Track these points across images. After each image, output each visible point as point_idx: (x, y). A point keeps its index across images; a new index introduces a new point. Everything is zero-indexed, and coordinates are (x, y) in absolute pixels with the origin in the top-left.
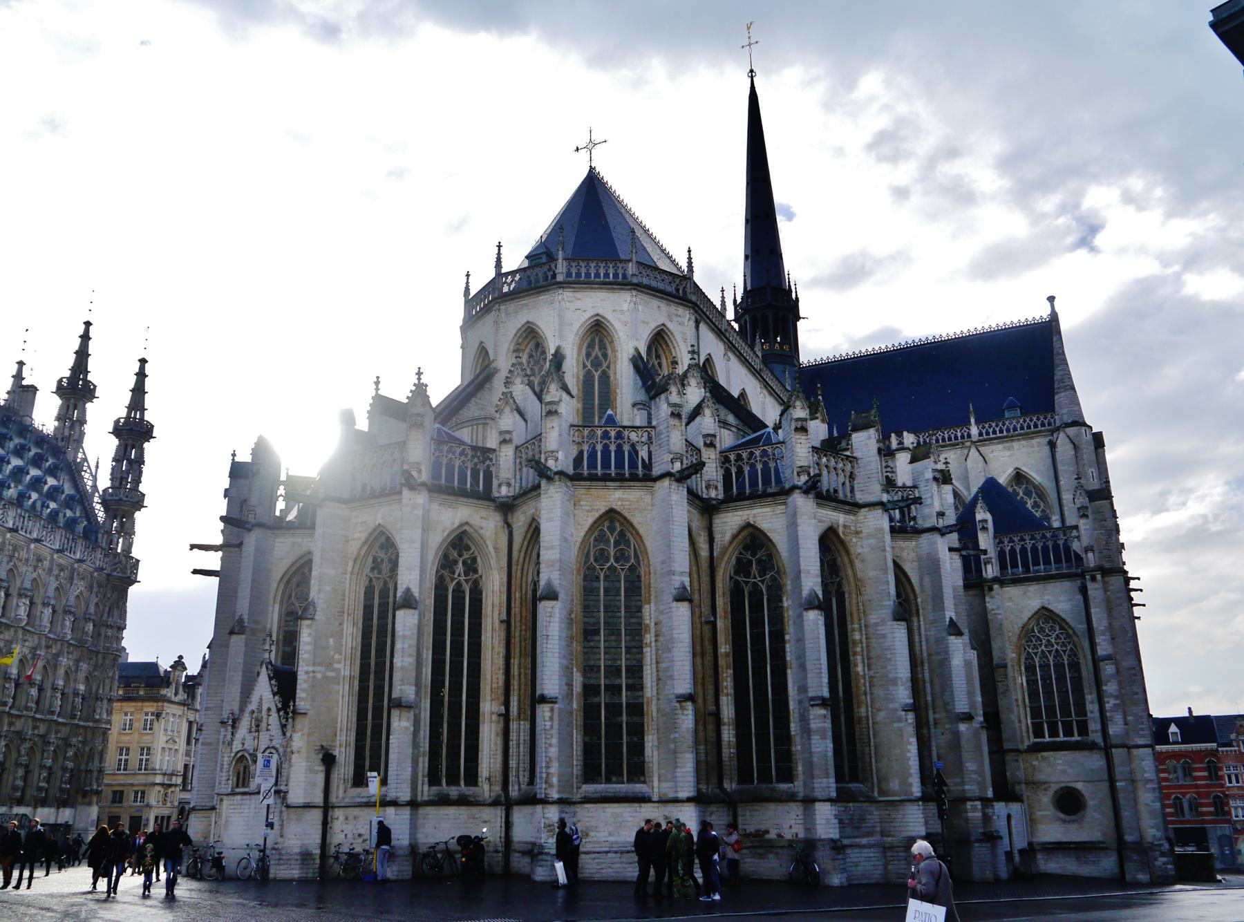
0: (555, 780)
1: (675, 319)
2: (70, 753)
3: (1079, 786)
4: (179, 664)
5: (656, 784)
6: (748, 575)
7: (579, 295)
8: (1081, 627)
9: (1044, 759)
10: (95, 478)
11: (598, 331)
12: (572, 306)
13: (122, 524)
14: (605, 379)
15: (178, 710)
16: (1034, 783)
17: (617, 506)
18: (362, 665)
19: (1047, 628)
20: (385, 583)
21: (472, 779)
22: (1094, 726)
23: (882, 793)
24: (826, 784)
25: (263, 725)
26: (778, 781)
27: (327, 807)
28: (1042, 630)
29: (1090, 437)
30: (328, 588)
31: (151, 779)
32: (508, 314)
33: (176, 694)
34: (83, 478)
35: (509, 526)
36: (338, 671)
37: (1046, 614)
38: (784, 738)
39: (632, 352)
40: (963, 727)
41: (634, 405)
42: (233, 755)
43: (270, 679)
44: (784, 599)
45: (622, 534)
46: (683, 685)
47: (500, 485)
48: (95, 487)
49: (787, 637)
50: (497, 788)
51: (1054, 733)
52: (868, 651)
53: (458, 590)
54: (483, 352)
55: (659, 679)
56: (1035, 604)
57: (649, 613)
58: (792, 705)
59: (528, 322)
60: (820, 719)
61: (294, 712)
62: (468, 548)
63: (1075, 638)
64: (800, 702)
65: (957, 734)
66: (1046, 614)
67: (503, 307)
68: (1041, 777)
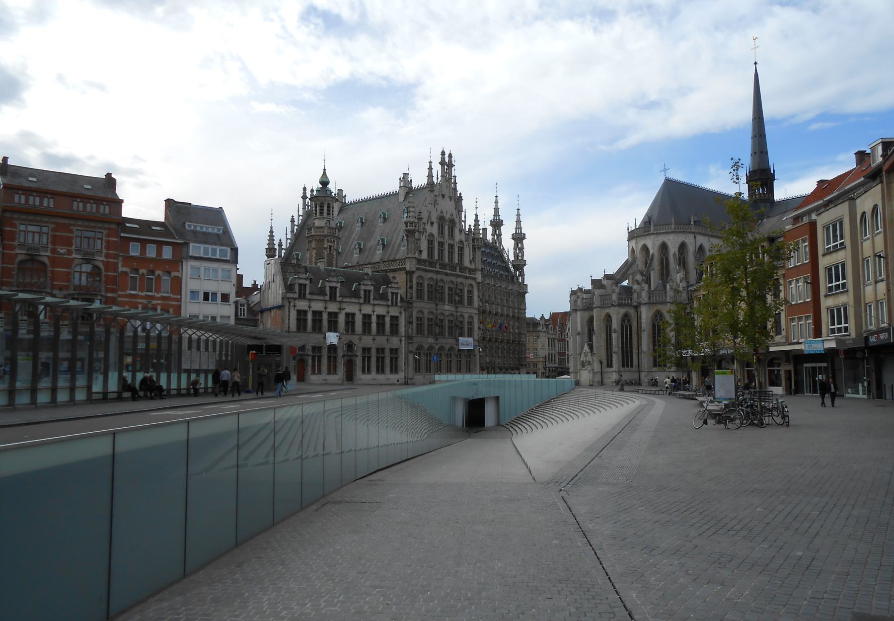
0: (646, 367)
2: (516, 353)
4: (542, 317)
7: (658, 236)
10: (508, 256)
11: (664, 247)
13: (520, 272)
14: (667, 259)
15: (544, 334)
17: (659, 309)
21: (632, 366)
27: (602, 372)
31: (538, 360)
33: (543, 329)
34: (504, 256)
39: (673, 252)
48: (508, 259)
50: (637, 368)
54: (633, 249)
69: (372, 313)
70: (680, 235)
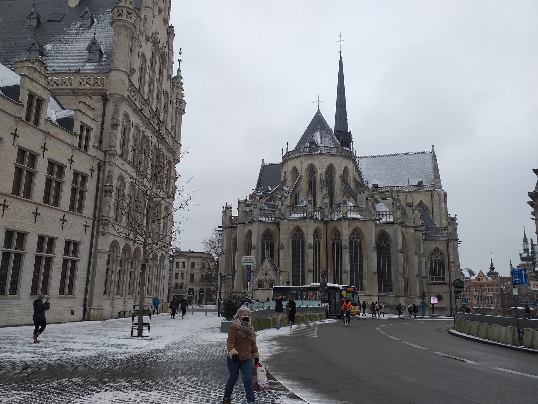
1: (349, 164)
3: (442, 294)
5: (367, 292)
6: (381, 242)
7: (326, 157)
8: (446, 253)
9: (433, 286)
12: (324, 160)
16: (430, 292)
17: (358, 226)
18: (262, 255)
19: (437, 253)
20: (298, 240)
22: (447, 279)
23: (410, 295)
24: (403, 293)
25: (268, 273)
26: (388, 291)
28: (435, 253)
29: (443, 193)
30: (286, 241)
32: (305, 160)
35: (327, 227)
36: (288, 261)
37: (437, 250)
38: (390, 281)
40: (424, 280)
41: (341, 190)
42: (257, 280)
43: (269, 262)
44: (391, 249)
45: (358, 233)
46: (375, 270)
47: (325, 217)
49: (392, 258)
51: (436, 280)
52: (408, 262)
53: (315, 243)
55: (368, 268)
56: (434, 246)
57: (364, 252)
58: (393, 274)
59: (311, 163)
60: (401, 279)
61: (280, 271)
62: (317, 232)
63: (444, 256)
64: (395, 274)
65: (423, 281)
66: (437, 250)
67: (303, 158)
68: (432, 291)
69: (40, 152)
70: (345, 160)
